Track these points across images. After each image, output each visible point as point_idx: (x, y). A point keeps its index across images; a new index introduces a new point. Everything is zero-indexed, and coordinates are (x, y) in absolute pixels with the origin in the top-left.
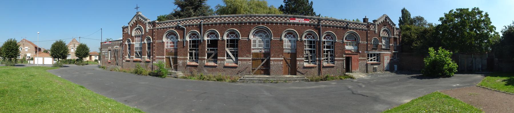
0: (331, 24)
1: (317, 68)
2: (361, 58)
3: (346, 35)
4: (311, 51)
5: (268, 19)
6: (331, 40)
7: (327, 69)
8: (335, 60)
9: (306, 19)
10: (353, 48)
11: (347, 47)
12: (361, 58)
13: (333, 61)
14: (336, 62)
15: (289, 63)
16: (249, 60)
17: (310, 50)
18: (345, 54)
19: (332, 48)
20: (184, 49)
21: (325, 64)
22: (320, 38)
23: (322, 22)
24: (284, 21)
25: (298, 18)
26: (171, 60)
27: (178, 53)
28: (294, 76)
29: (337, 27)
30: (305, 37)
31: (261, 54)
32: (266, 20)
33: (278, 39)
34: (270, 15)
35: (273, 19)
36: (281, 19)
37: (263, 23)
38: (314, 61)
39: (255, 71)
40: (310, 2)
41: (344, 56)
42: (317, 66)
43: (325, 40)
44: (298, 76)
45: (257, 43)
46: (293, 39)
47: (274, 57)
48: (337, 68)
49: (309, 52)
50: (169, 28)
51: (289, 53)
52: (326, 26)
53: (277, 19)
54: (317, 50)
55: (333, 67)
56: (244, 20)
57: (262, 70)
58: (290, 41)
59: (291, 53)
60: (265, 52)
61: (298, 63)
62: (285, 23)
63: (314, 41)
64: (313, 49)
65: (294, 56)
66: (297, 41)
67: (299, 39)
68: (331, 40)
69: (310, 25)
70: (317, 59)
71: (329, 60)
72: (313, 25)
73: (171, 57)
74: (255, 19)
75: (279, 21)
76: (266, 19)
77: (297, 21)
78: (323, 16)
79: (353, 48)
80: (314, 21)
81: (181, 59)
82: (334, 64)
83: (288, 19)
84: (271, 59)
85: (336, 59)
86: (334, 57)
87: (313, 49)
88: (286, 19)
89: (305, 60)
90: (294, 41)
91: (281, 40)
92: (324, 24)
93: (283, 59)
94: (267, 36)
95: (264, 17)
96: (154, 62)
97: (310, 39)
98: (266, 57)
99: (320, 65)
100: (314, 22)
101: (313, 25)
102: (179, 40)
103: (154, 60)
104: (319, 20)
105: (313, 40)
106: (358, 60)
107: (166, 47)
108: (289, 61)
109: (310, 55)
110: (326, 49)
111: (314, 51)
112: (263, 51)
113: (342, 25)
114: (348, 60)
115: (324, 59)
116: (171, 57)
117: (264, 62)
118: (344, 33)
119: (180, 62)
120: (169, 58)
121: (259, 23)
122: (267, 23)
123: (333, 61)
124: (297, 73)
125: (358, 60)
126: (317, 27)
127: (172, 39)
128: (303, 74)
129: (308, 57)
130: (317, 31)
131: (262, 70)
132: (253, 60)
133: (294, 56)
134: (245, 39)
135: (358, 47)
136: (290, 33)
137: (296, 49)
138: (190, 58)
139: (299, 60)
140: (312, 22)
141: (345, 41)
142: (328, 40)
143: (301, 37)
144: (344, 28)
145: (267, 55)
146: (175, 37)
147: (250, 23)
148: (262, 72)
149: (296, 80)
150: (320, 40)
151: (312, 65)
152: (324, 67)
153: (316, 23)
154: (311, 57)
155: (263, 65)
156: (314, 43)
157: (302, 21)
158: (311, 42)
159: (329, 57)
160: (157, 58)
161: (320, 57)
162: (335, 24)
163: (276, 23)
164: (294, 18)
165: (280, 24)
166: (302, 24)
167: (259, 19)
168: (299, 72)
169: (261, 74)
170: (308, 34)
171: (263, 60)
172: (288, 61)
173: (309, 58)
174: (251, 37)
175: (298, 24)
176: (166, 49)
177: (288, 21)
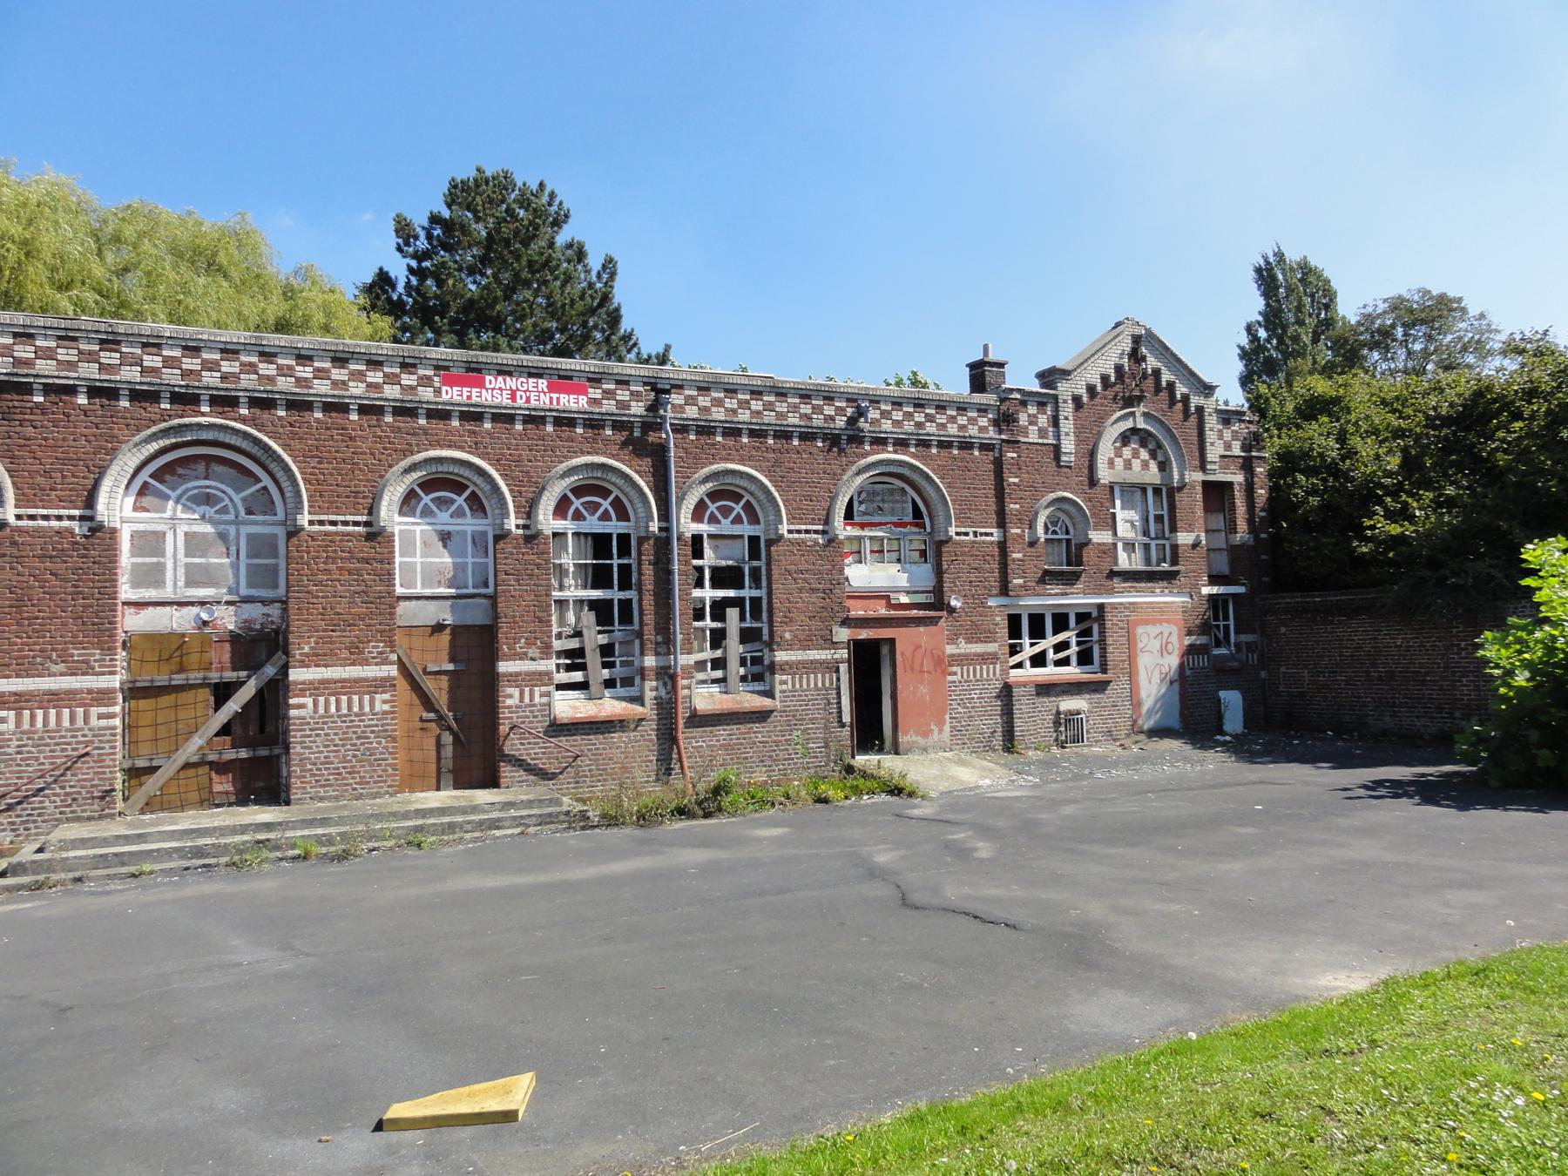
0: (744, 416)
1: (650, 730)
2: (964, 647)
3: (851, 485)
4: (602, 611)
5: (267, 369)
6: (747, 530)
7: (722, 732)
8: (772, 668)
9: (563, 382)
10: (903, 580)
11: (860, 575)
12: (964, 647)
13: (759, 672)
14: (782, 683)
15: (441, 696)
16: (102, 697)
17: (594, 605)
18: (846, 622)
19: (756, 583)
21: (704, 697)
22: (665, 515)
23: (676, 398)
24: (392, 392)
25: (504, 371)
28: (483, 796)
29: (784, 435)
30: (561, 508)
31: (205, 643)
32: (248, 381)
33: (349, 523)
34: (282, 340)
35: (305, 372)
36: (375, 377)
37: (225, 402)
38: (628, 682)
39: (152, 784)
40: (595, 262)
41: (843, 634)
42: (648, 710)
43: (703, 528)
44: (516, 789)
45: (170, 560)
46: (470, 524)
47: (316, 659)
48: (794, 720)
49: (589, 617)
51: (438, 628)
52: (706, 430)
53: (338, 374)
54: (649, 601)
55: (762, 716)
56: (44, 367)
57: (220, 768)
58: (445, 537)
59: (457, 630)
60: (247, 624)
61: (510, 697)
62: (405, 411)
63: (624, 539)
64: (615, 594)
65: (476, 647)
66: (502, 536)
67: (512, 523)
68: (747, 530)
69: (594, 424)
70: (650, 661)
71: (735, 670)
72: (618, 426)
74: (151, 361)
75: (357, 389)
76: (251, 368)
77: (494, 392)
78: (682, 363)
79: (903, 580)
80: (623, 395)
82: (770, 694)
83: (426, 381)
84: (295, 675)
85: (781, 656)
86: (770, 645)
87: (615, 594)
88: (408, 380)
89: (564, 677)
90: (479, 540)
91: (375, 534)
92: (692, 412)
93: (393, 671)
94: (261, 504)
95: (229, 351)
97: (593, 524)
98: (254, 668)
99: (667, 709)
100: (623, 405)
101: (618, 426)
104: (659, 391)
105: (614, 527)
106: (944, 665)
108: (439, 690)
109: (594, 638)
110: (708, 594)
111: (626, 605)
112: (227, 619)
113: (818, 421)
114: (869, 664)
115: (700, 665)
117: (233, 706)
118: (837, 478)
121: (185, 400)
122: (255, 403)
123: (759, 672)
124: (506, 771)
125: (944, 665)
126: (644, 441)
128: (545, 775)
129: (580, 652)
130: (646, 463)
131: (220, 768)
132: (134, 692)
133: (476, 647)
134: (63, 519)
135: (939, 573)
136: (441, 484)
137: (493, 598)
139: (514, 678)
140: (609, 406)
141: (842, 530)
142: (726, 527)
143: (529, 510)
144: (833, 440)
145: (261, 647)
147: (104, 392)
148: (223, 785)
149: (495, 824)
150: (666, 529)
151: (610, 706)
152: (698, 720)
153: (638, 408)
154: (606, 650)
155: (225, 730)
156: (624, 550)
157: (536, 394)
158: (600, 544)
159: (734, 648)
161: (666, 644)
162: (769, 417)
163: (328, 407)
164: (473, 373)
165: (364, 410)
166: (534, 420)
167: (191, 363)
168: (519, 763)
169: (209, 801)
170: (578, 491)
171: (223, 692)
172: (429, 684)
173: (593, 659)
174: (116, 505)
175: (503, 418)
177: (426, 394)
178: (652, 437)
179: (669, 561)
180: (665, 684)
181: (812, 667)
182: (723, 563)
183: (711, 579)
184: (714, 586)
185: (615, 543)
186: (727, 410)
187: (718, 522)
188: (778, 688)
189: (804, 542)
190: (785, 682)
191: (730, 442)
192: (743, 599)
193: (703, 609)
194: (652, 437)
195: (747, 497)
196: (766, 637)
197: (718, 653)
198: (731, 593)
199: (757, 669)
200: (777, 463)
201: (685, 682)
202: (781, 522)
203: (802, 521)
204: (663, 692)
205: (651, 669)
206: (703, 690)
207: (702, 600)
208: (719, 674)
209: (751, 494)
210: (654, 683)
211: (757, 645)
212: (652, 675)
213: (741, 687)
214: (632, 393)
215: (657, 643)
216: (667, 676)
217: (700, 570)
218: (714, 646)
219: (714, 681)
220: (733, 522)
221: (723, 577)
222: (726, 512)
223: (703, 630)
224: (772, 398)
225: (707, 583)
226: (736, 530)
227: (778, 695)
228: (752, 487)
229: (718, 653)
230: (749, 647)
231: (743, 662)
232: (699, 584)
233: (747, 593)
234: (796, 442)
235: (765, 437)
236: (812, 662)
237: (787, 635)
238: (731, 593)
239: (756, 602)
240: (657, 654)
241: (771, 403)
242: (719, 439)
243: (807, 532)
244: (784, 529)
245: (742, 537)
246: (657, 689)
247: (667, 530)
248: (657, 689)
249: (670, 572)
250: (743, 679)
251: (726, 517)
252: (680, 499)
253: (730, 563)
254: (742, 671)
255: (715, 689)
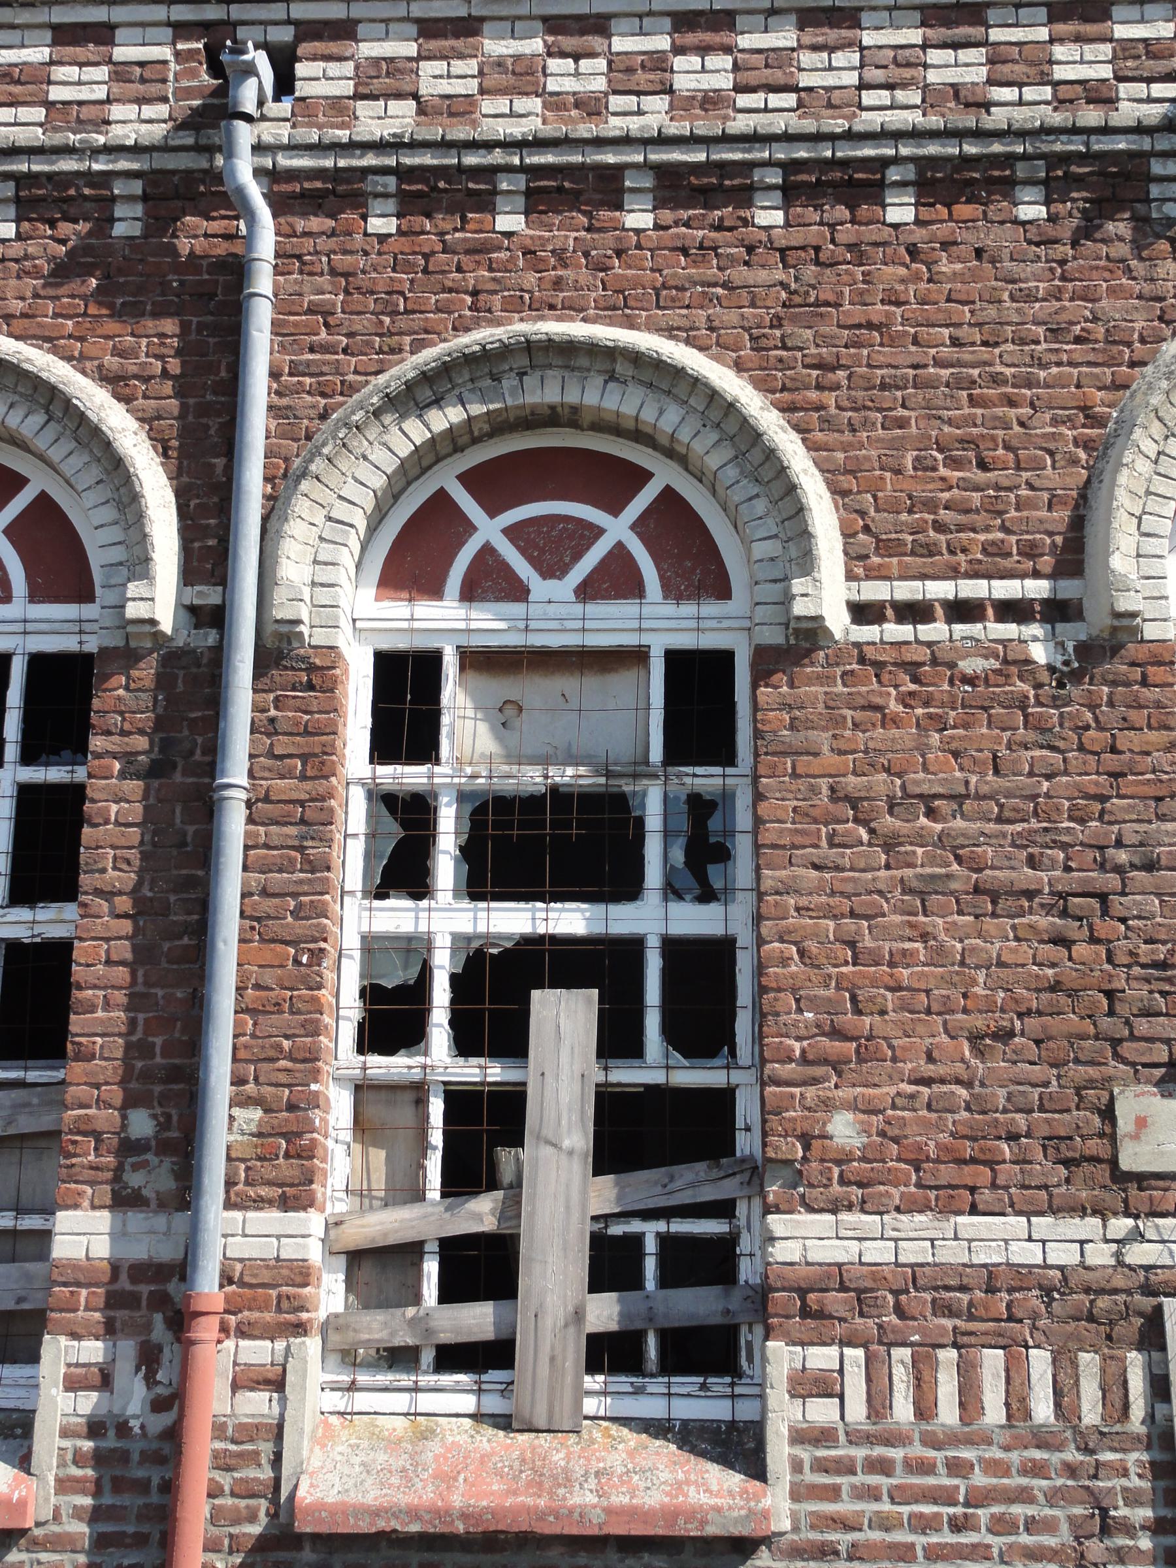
13: (688, 1327)
29: (838, 181)
43: (442, 620)
52: (444, 187)
68: (662, 623)
71: (557, 1292)
82: (739, 1446)
110: (450, 920)
123: (688, 1327)
130: (154, 343)
142: (554, 612)
159: (560, 1192)
161: (162, 1165)
178: (194, 236)
179: (210, 760)
180: (149, 1359)
181: (988, 1307)
182: (531, 779)
183: (469, 852)
184: (481, 883)
185: (14, 696)
186: (555, 103)
187: (518, 592)
188: (784, 1415)
189: (940, 659)
190: (825, 1386)
191: (565, 232)
192: (633, 947)
193: (420, 989)
194: (194, 236)
195: (665, 475)
196: (746, 1144)
197: (480, 1214)
198: (571, 920)
199: (696, 1304)
200: (799, 305)
201: (259, 1352)
202: (806, 562)
203: (926, 558)
204: (134, 1398)
205: (79, 1275)
206: (386, 1401)
207: (416, 949)
208: (476, 1320)
209: (672, 453)
210: (93, 1350)
211: (693, 1181)
212: (87, 1305)
213: (597, 1394)
214: (120, 72)
215: (128, 1148)
216: (152, 1304)
217: (411, 814)
218: (467, 1174)
219: (453, 1357)
220: (586, 591)
221: (518, 845)
222: (553, 547)
223: (418, 1091)
224: (784, 37)
225: (446, 867)
226: (610, 624)
227: (779, 1451)
228: (668, 419)
229: (480, 1214)
230: (646, 1186)
231: (611, 1263)
232: (404, 873)
233: (650, 918)
234: (900, 210)
235: (745, 196)
236: (991, 1278)
237: (844, 1130)
238: (571, 920)
239: (702, 968)
240: (123, 1200)
241: (775, 57)
242: (510, 221)
243: (962, 611)
244: (828, 594)
245: (638, 656)
246: (105, 1379)
247: (214, 618)
248: (105, 1379)
249: (205, 807)
250: (610, 1354)
251: (552, 570)
252: (283, 482)
253: (566, 775)
254: (604, 1312)
255: (454, 1396)
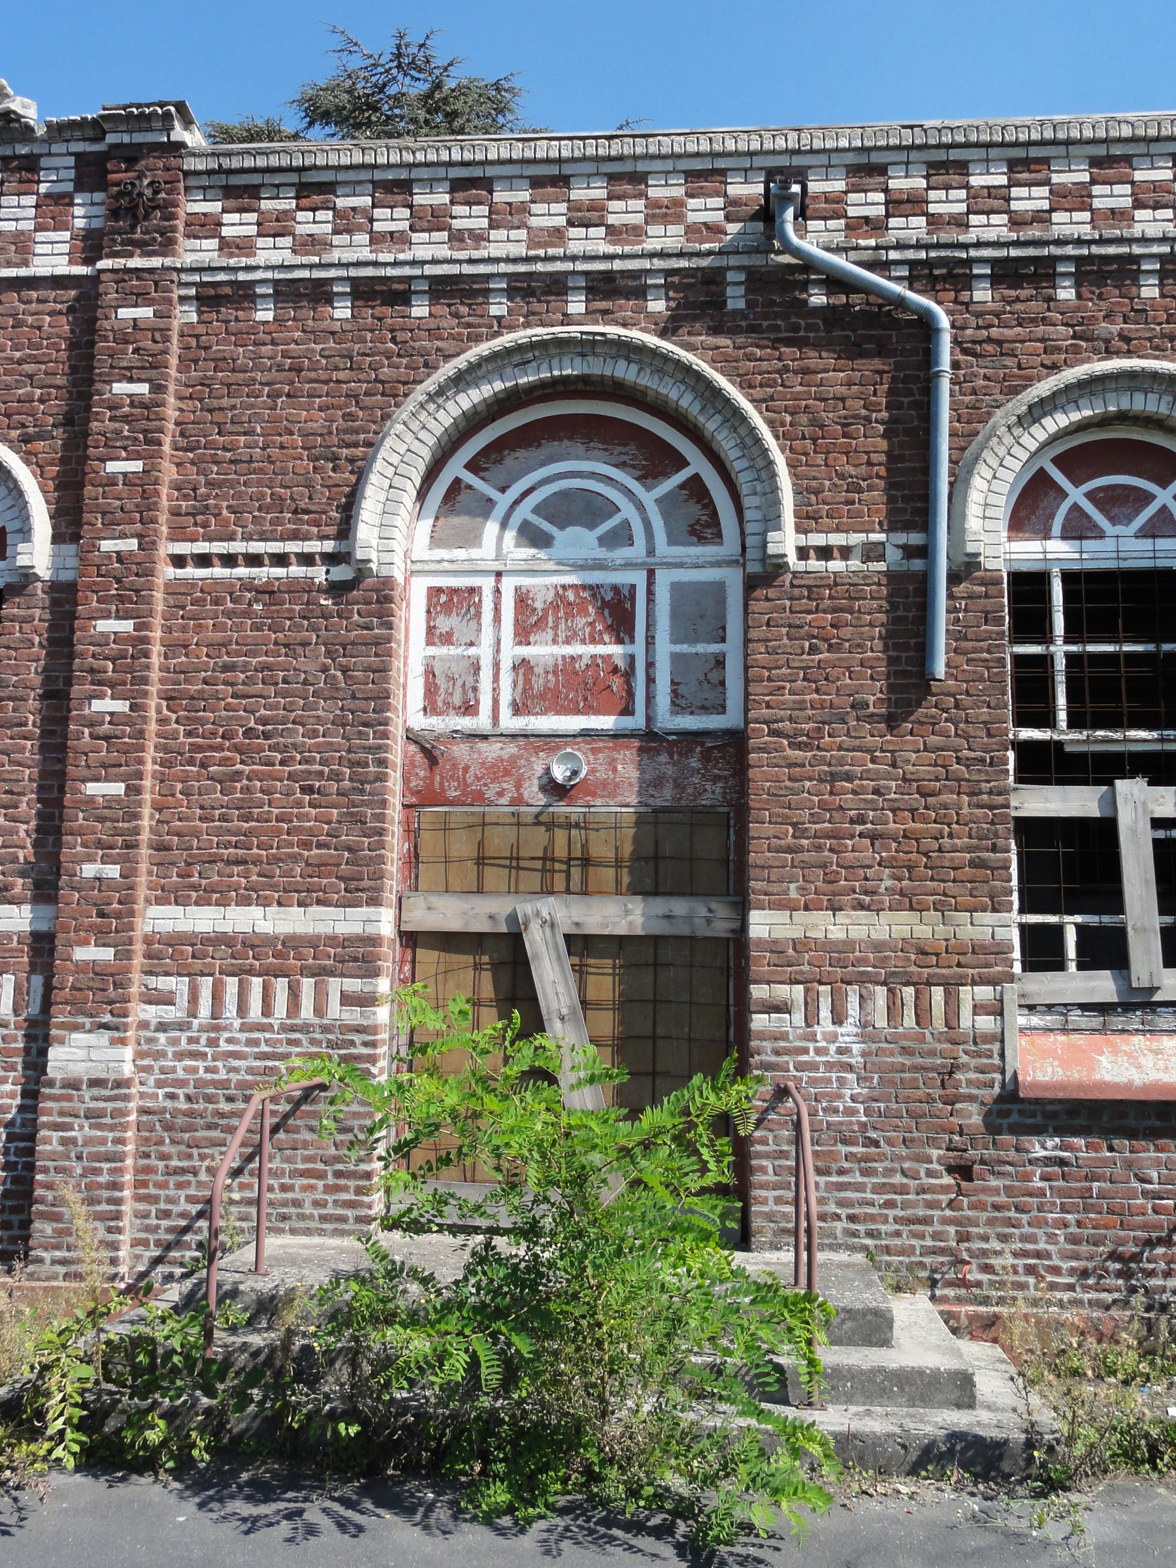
20: (913, 751)
26: (552, 979)
27: (763, 831)
50: (537, 289)
73: (548, 922)
81: (835, 971)
96: (73, 1054)
102: (786, 541)
103: (105, 999)
107: (410, 710)
116: (548, 922)
119: (818, 1040)
120: (506, 955)
127: (578, 541)
138: (1042, 951)
146: (640, 502)
160: (177, 953)
176: (428, 751)
